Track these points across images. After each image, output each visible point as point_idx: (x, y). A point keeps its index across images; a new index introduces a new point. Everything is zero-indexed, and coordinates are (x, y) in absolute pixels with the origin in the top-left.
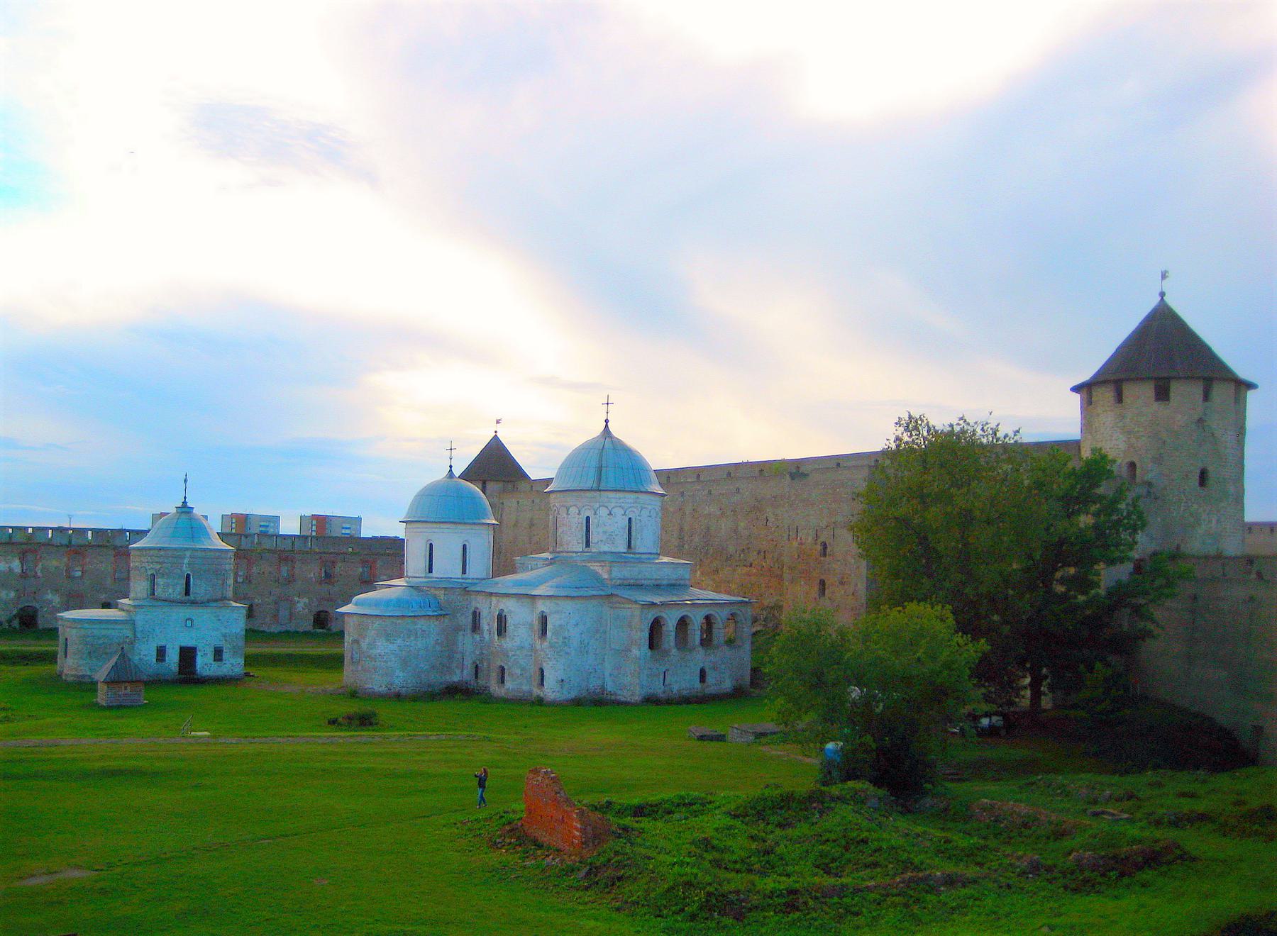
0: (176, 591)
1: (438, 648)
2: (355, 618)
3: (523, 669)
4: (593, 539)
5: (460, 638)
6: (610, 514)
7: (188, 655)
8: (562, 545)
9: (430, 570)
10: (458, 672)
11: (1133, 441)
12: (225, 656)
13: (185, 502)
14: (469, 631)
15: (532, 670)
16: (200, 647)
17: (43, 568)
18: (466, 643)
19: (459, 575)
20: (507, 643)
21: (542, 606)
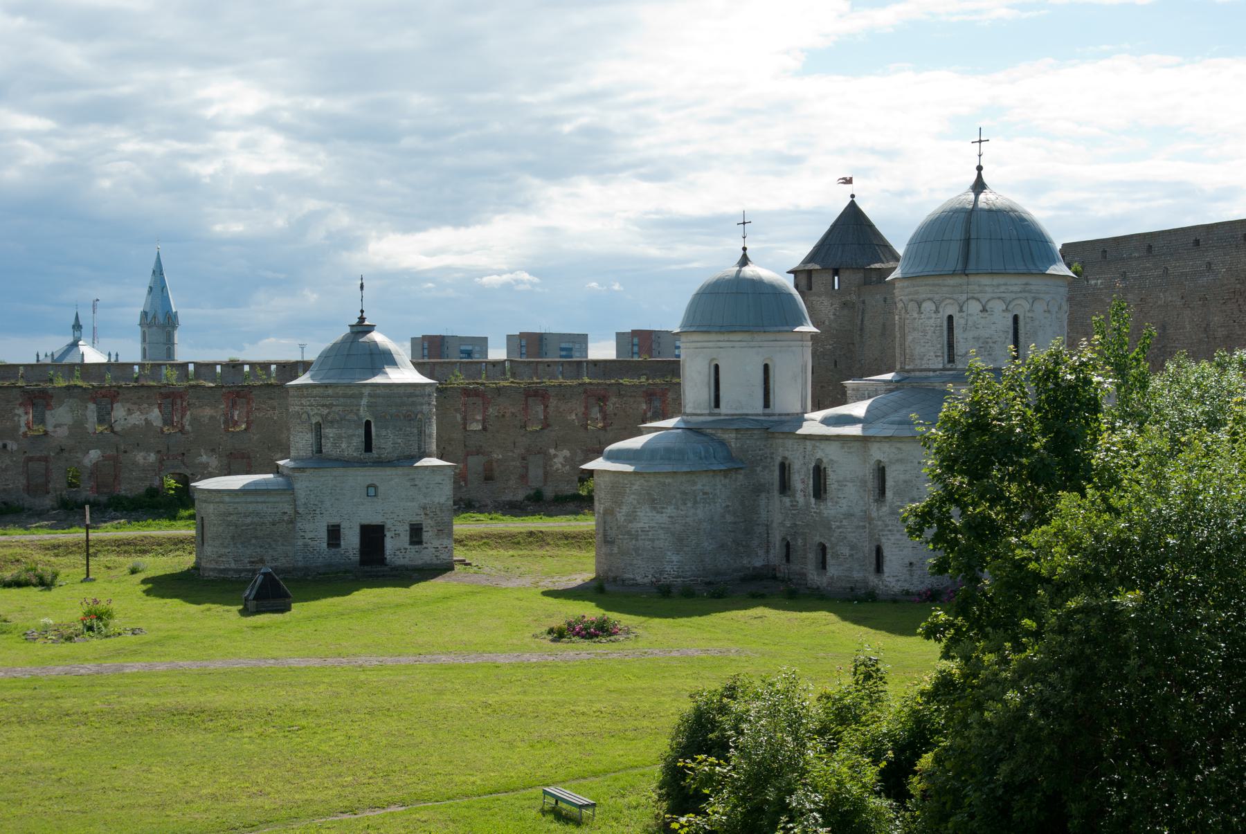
0: (351, 445)
1: (729, 518)
2: (607, 479)
3: (853, 547)
4: (960, 348)
5: (763, 502)
6: (984, 310)
7: (373, 536)
8: (912, 360)
9: (717, 405)
10: (761, 552)
12: (426, 536)
13: (362, 319)
14: (776, 493)
15: (868, 548)
16: (387, 526)
17: (195, 420)
18: (775, 511)
19: (756, 406)
20: (829, 509)
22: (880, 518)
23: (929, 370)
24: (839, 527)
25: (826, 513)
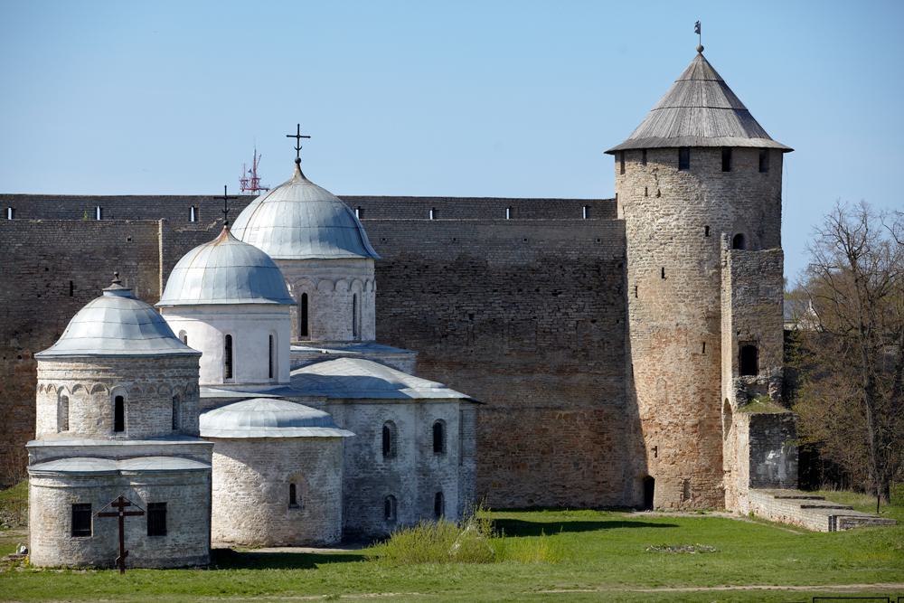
2: (294, 445)
11: (741, 212)
21: (437, 414)
22: (440, 469)
23: (343, 342)
24: (405, 480)
25: (396, 468)
